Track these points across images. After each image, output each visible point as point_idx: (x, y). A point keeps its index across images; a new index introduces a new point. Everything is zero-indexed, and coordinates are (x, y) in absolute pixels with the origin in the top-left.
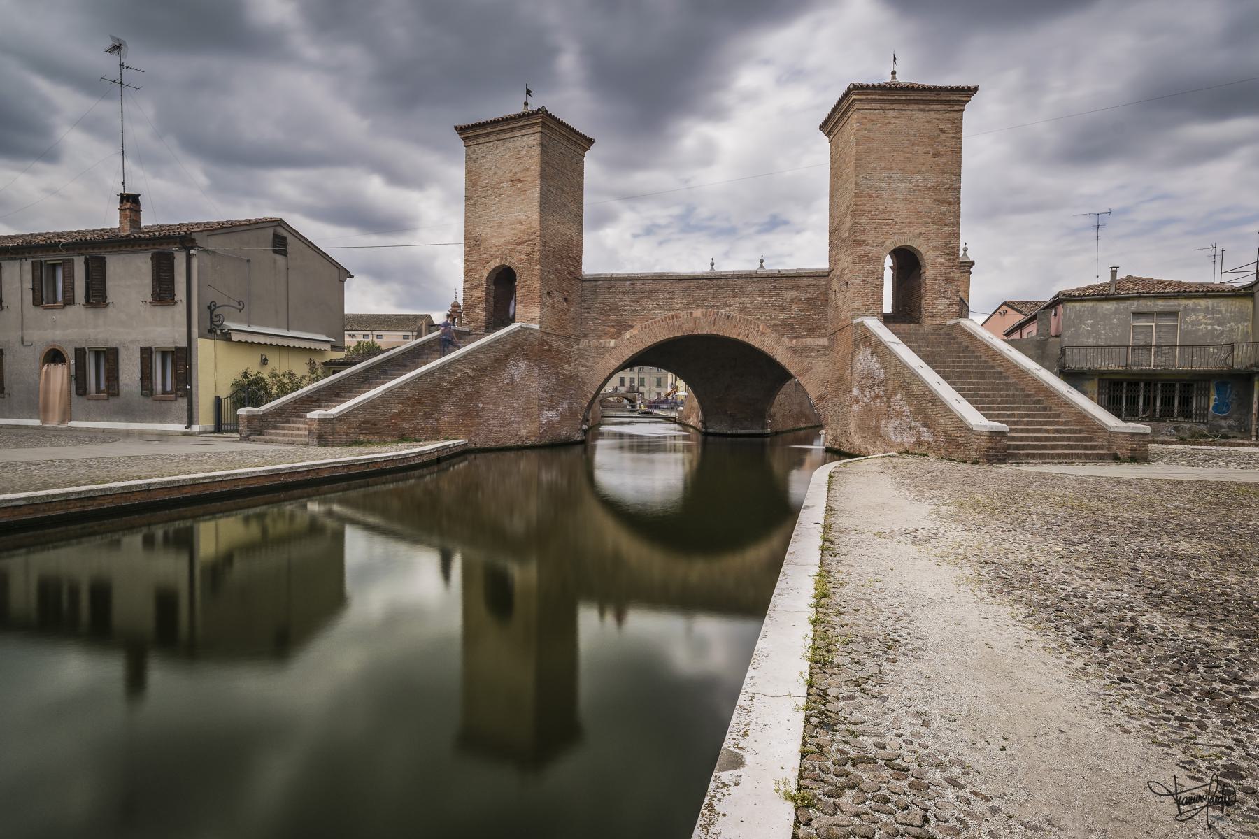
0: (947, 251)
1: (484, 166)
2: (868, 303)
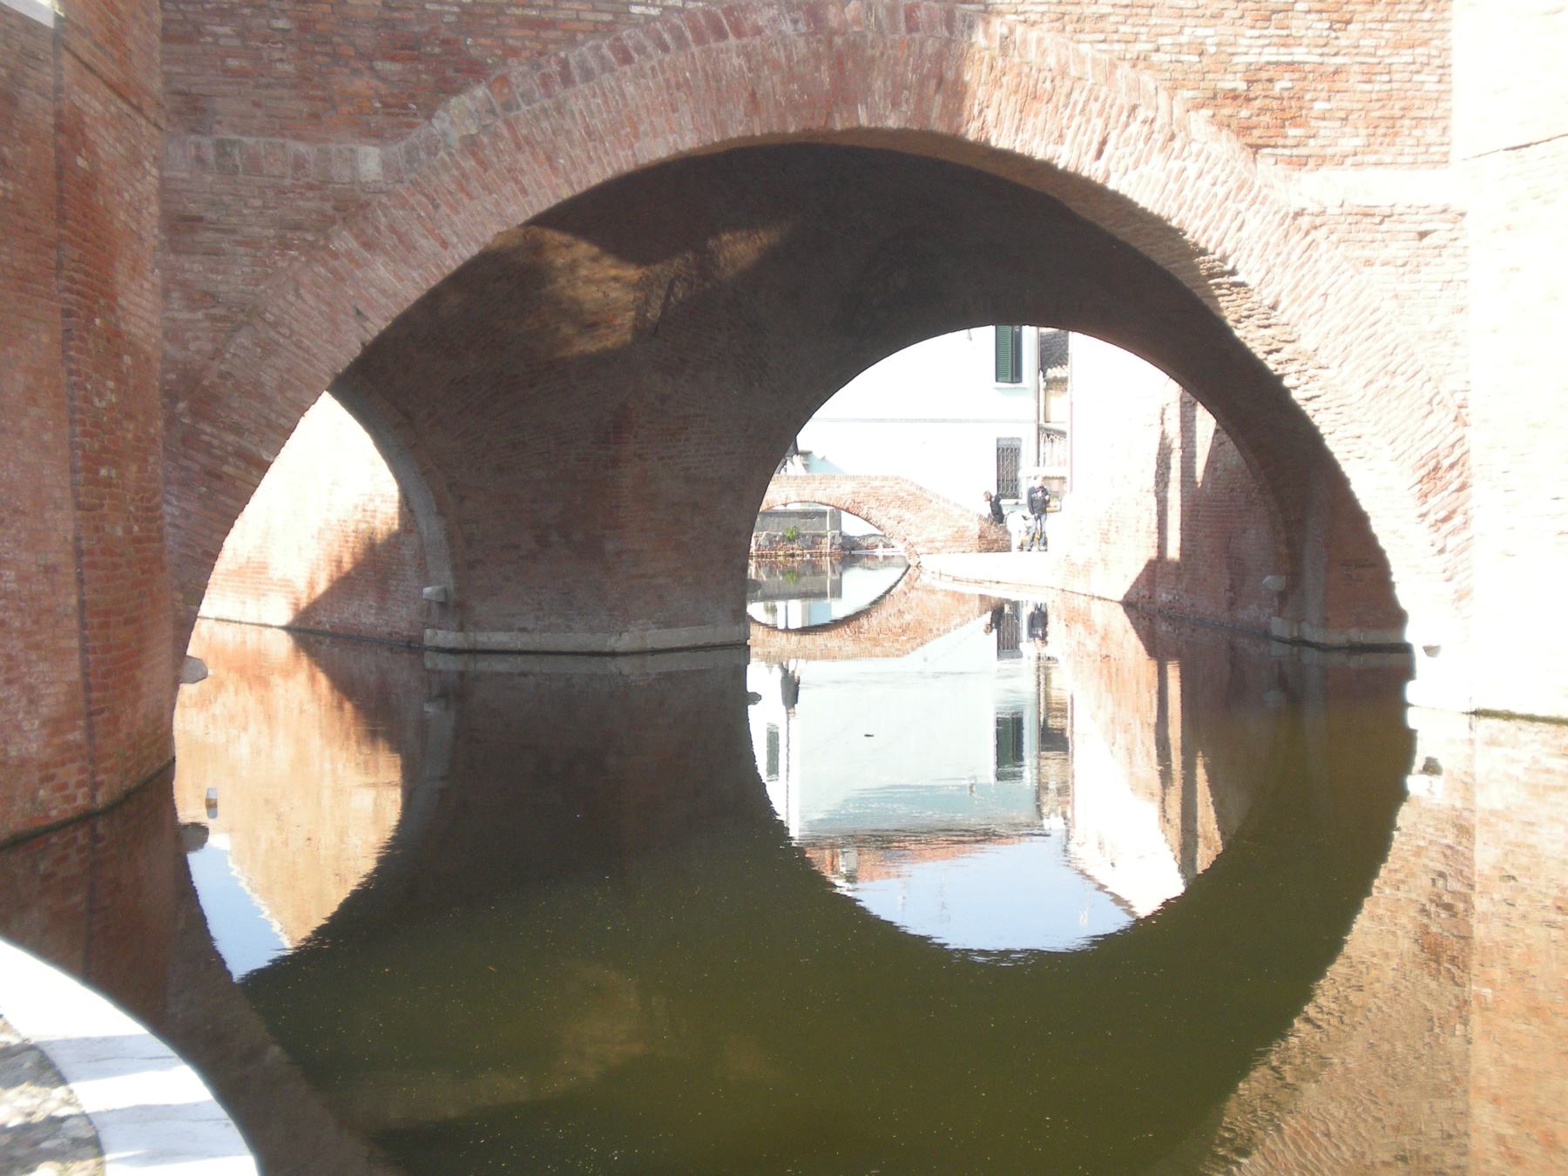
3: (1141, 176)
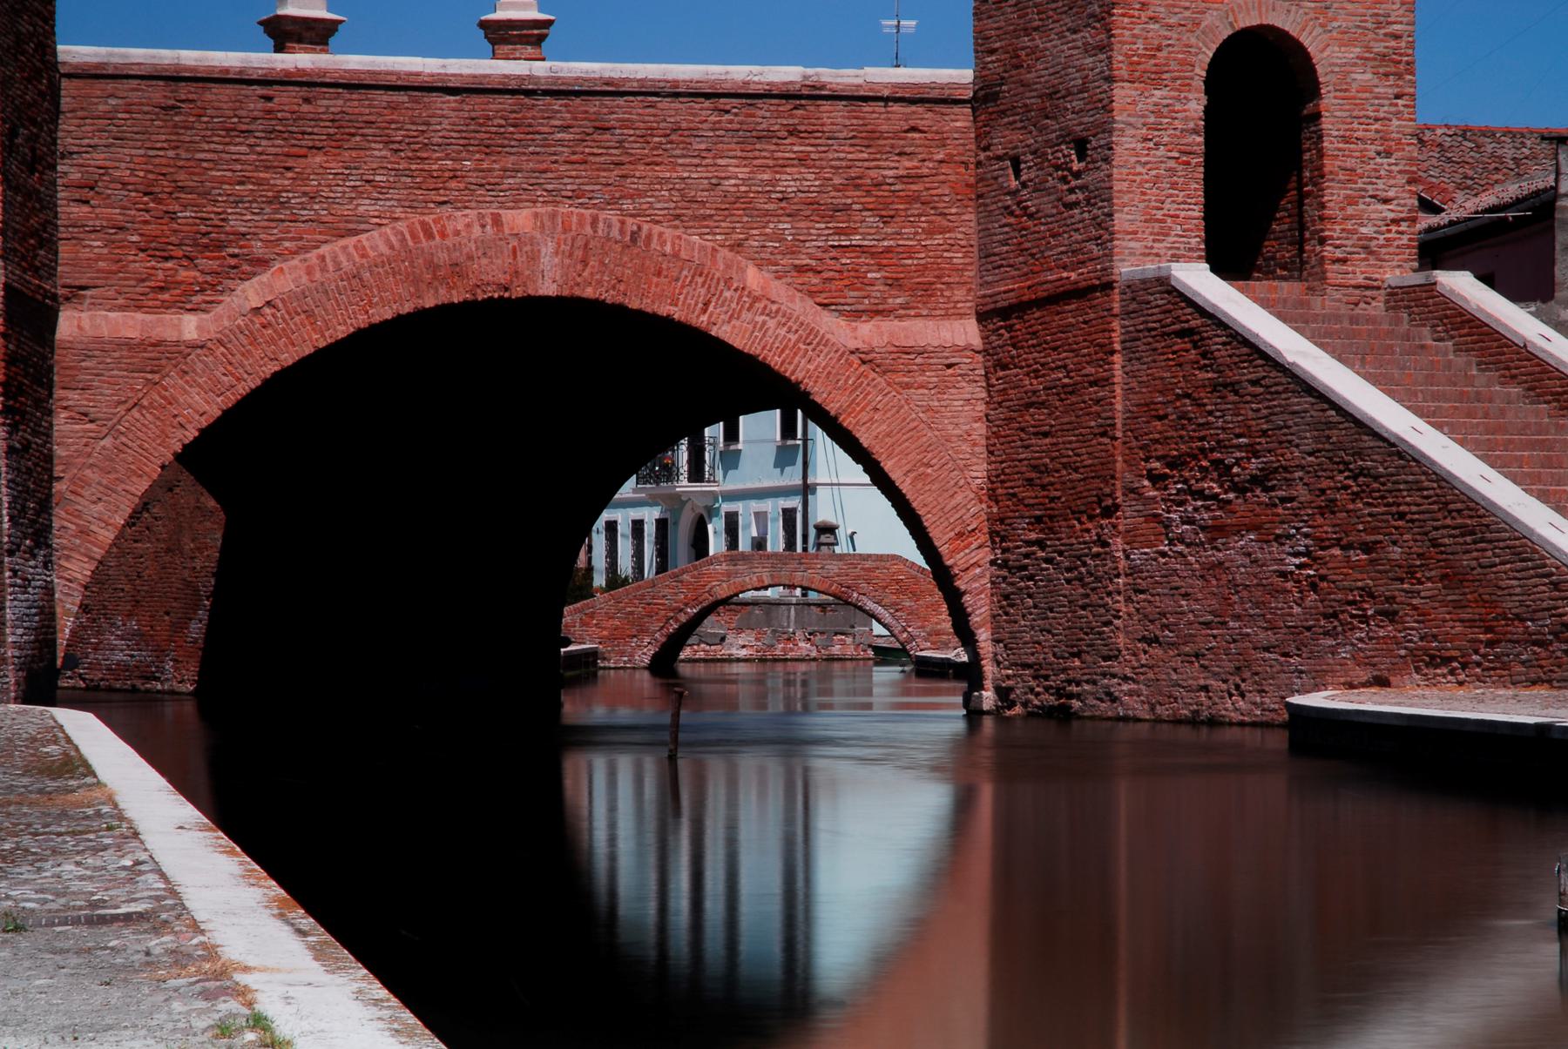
0: (1379, 47)
2: (1159, 214)
3: (734, 327)
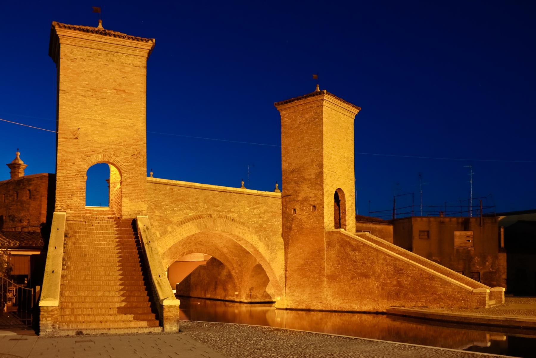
1: (83, 68)
